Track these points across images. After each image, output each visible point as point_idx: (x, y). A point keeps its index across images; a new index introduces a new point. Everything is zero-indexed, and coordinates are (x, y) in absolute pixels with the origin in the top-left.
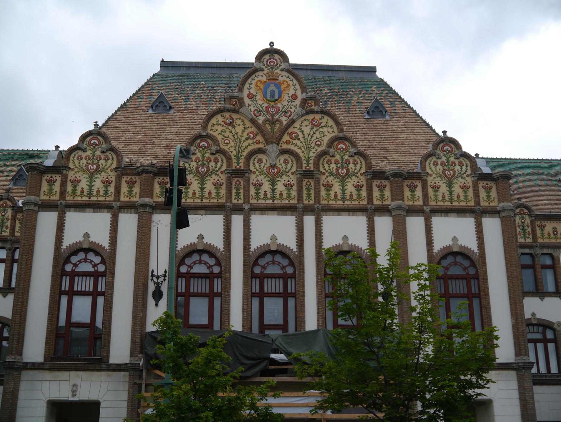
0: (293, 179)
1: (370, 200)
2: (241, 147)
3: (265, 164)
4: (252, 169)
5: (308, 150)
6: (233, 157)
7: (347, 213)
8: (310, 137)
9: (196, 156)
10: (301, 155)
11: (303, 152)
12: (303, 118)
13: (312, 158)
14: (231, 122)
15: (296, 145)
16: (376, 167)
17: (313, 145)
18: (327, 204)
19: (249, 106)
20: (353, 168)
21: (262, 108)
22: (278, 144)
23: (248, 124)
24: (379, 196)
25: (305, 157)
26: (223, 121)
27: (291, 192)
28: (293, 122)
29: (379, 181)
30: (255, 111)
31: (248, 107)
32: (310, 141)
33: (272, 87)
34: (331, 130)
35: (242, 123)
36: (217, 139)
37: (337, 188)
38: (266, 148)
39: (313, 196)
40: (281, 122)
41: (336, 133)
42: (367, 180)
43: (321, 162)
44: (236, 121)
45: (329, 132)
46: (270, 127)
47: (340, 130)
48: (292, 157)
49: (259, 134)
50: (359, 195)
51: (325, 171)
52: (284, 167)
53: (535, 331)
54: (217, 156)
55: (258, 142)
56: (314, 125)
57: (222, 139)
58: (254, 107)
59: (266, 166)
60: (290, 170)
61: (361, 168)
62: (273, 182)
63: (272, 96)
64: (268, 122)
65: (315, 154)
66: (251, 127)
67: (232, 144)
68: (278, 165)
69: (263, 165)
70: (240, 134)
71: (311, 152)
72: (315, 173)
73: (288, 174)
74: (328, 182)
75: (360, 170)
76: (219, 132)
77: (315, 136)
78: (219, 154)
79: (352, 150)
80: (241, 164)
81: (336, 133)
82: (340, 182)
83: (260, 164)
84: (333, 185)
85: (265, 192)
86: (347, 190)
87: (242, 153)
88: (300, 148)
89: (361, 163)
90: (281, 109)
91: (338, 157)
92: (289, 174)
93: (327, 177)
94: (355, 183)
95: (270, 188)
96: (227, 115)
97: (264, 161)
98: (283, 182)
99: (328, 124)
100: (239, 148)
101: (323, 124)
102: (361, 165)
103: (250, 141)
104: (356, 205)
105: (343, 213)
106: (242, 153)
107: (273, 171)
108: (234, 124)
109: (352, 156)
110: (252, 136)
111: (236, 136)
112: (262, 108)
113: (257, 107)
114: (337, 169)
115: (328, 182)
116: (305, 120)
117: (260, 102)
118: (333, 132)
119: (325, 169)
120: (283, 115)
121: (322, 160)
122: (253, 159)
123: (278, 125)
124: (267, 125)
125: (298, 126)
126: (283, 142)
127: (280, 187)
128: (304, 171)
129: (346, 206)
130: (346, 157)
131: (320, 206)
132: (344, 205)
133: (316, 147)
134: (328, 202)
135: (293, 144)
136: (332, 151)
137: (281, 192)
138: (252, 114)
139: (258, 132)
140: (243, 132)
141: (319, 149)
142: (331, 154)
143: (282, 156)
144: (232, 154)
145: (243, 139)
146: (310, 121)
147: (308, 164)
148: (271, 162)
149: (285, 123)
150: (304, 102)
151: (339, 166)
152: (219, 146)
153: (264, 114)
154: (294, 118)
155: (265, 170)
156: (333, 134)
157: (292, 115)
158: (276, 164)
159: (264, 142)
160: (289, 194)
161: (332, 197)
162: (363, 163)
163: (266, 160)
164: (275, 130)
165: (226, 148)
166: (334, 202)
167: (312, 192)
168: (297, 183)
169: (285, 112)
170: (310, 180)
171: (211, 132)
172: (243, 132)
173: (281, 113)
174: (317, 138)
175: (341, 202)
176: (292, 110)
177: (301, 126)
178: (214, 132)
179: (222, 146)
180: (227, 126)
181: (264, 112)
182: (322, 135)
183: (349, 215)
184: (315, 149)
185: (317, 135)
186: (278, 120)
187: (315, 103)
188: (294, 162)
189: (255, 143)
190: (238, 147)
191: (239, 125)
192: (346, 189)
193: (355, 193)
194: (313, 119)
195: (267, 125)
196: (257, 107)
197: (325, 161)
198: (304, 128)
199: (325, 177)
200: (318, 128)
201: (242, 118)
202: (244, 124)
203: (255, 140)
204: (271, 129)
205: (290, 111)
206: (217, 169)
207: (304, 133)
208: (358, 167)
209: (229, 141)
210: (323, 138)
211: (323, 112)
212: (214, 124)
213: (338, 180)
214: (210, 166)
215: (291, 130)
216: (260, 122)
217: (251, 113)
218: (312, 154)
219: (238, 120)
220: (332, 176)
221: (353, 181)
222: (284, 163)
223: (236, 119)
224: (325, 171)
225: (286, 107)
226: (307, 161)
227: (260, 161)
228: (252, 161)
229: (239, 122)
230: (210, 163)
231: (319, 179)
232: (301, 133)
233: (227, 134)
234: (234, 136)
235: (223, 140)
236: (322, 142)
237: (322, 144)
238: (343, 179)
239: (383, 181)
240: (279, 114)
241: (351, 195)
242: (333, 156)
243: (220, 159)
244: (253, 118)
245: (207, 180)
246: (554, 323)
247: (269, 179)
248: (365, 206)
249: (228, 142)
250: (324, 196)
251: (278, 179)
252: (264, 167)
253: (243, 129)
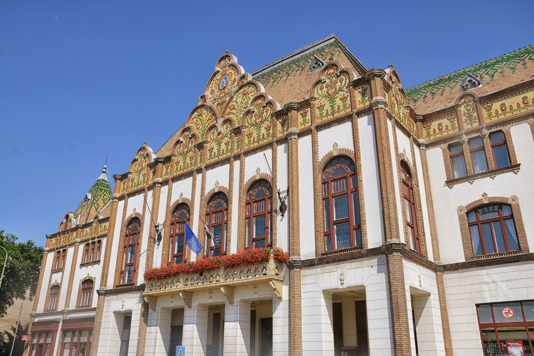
8: (241, 104)
28: (232, 98)
53: (495, 210)
103: (209, 122)
116: (239, 94)
118: (255, 94)
220: (252, 127)
246: (508, 198)
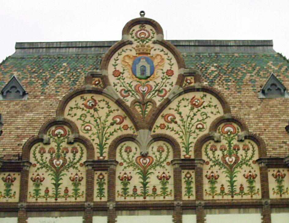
0: (169, 171)
1: (265, 192)
2: (105, 134)
3: (135, 154)
4: (119, 159)
5: (188, 135)
6: (95, 146)
7: (237, 210)
8: (189, 119)
9: (49, 146)
10: (179, 141)
11: (181, 137)
12: (181, 97)
13: (193, 145)
14: (92, 105)
15: (173, 130)
16: (271, 153)
17: (193, 129)
18: (212, 200)
19: (115, 85)
21: (131, 87)
22: (150, 129)
23: (114, 106)
24: (276, 189)
25: (184, 143)
26: (83, 104)
27: (167, 186)
28: (168, 102)
29: (276, 170)
30: (122, 90)
31: (114, 86)
32: (190, 124)
33: (143, 62)
34: (215, 111)
35: (107, 105)
36: (75, 125)
37: (223, 179)
38: (136, 134)
39: (194, 190)
40: (154, 103)
41: (222, 114)
42: (261, 169)
43: (203, 149)
44: (99, 103)
45: (212, 113)
46: (140, 110)
47: (226, 109)
48: (168, 144)
49: (127, 118)
50: (251, 188)
51: (208, 160)
52: (158, 156)
54: (76, 145)
55: (126, 128)
56: (195, 104)
57: (82, 125)
58: (121, 86)
59: (136, 156)
60: (165, 160)
61: (253, 154)
62: (145, 175)
63: (143, 71)
64: (138, 104)
65: (196, 140)
66: (118, 110)
67: (95, 130)
68: (150, 154)
69: (131, 154)
70: (103, 118)
71: (191, 138)
72: (196, 162)
73: (163, 165)
74: (212, 172)
75: (252, 157)
76: (78, 116)
77: (195, 118)
78: (78, 143)
79: (242, 134)
80: (106, 155)
81: (222, 114)
82: (227, 173)
83: (128, 153)
84: (218, 176)
85: (135, 187)
86: (236, 182)
87: (106, 141)
88: (177, 133)
89: (253, 148)
90: (154, 87)
91: (224, 142)
92: (165, 164)
93: (212, 166)
95: (141, 182)
96: (88, 96)
97: (134, 150)
98: (70, 175)
99: (211, 104)
100: (102, 134)
101: (205, 104)
102: (254, 151)
103: (116, 127)
104: (248, 200)
105: (231, 210)
106: (106, 141)
107: (145, 161)
108: (97, 107)
109: (241, 141)
110: (118, 120)
111: (98, 121)
112: (131, 87)
113: (124, 86)
114: (224, 157)
115: (212, 172)
116: (183, 99)
117: (128, 81)
118: (218, 112)
119: (209, 158)
120: (156, 94)
121: (204, 146)
122: (119, 147)
123: (150, 107)
124: (137, 107)
125: (175, 107)
126: (157, 126)
127: (153, 181)
128: (182, 160)
129: (236, 201)
130: (235, 142)
131: (203, 202)
132: (232, 200)
133: (197, 131)
134: (213, 197)
135: (168, 128)
136: (217, 135)
137: (154, 186)
138: (119, 94)
139: (126, 115)
140: (108, 116)
141: (202, 134)
142: (216, 139)
143: (155, 143)
144: (94, 143)
145: (108, 124)
146: (190, 100)
147: (187, 152)
148: (142, 151)
149: (158, 104)
150: (181, 79)
151: (225, 153)
152: (78, 133)
153: (133, 94)
154: (170, 98)
155: (134, 161)
156: (218, 115)
157: (168, 94)
158: (148, 153)
159: (133, 127)
160: (164, 189)
161: (218, 190)
162: (256, 148)
163: (136, 148)
164: (147, 113)
165: (87, 136)
166: (220, 197)
167: (193, 185)
168: (174, 176)
169: (159, 91)
170: (191, 171)
171: (69, 118)
172: (108, 116)
173: (154, 92)
174: (198, 121)
175: (229, 197)
176: (167, 89)
177: (178, 107)
178: (72, 117)
179: (81, 134)
180: (88, 110)
181: (133, 92)
182: (205, 117)
183: (239, 213)
184: (196, 134)
185: (199, 117)
186: (150, 101)
187: (195, 79)
188: (171, 150)
189: (122, 129)
190: (101, 134)
191: (103, 108)
192: (235, 181)
193: (246, 185)
194: (193, 98)
195: (137, 107)
196: (124, 86)
197: (209, 147)
198: (181, 109)
199: (209, 166)
200: (199, 108)
201: (106, 99)
202: (109, 107)
203: (122, 125)
204: (142, 111)
205: (165, 90)
206: (75, 161)
207: (182, 115)
208: (250, 153)
209: (91, 127)
210: (205, 121)
211: (204, 90)
212: (72, 108)
213: (225, 170)
214: (67, 158)
215: (165, 112)
216: (129, 104)
217: (118, 93)
218: (193, 140)
219: (102, 102)
220: (217, 166)
221: (243, 171)
222: (158, 151)
223: (99, 101)
224: (208, 160)
225: (159, 85)
226: (186, 148)
227: (128, 150)
228: (118, 150)
229: (102, 104)
230: (67, 154)
231: (201, 170)
232: (179, 115)
233: (88, 118)
234: (96, 121)
235: (83, 127)
236: (204, 125)
237: (205, 127)
238: (231, 169)
239: (281, 170)
240: (151, 94)
241: (242, 188)
242: (218, 141)
243: (79, 150)
244: (119, 99)
245: (63, 175)
247: (139, 171)
248: (259, 201)
249: (89, 128)
250: (208, 190)
251: (150, 171)
252: (133, 157)
253: (108, 112)
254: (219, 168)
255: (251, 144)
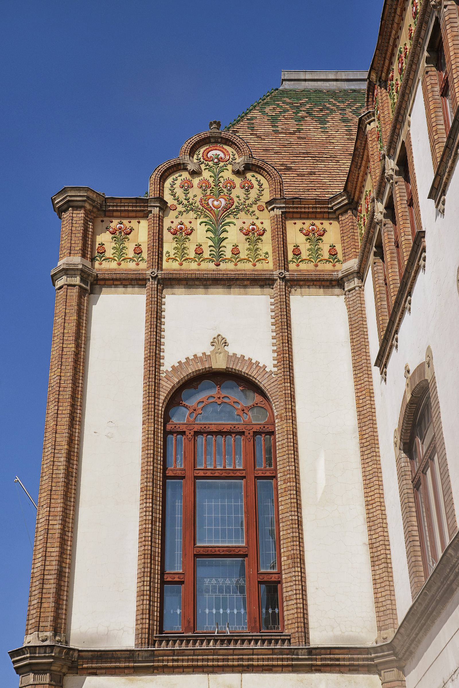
20: (242, 196)
74: (181, 223)
79: (240, 160)
86: (226, 241)
89: (261, 186)
91: (206, 174)
94: (246, 226)
242: (195, 173)
254: (195, 216)
255: (256, 178)
